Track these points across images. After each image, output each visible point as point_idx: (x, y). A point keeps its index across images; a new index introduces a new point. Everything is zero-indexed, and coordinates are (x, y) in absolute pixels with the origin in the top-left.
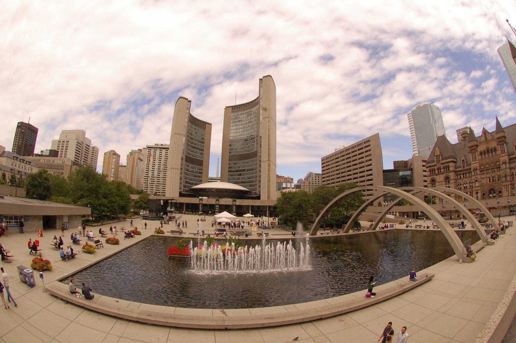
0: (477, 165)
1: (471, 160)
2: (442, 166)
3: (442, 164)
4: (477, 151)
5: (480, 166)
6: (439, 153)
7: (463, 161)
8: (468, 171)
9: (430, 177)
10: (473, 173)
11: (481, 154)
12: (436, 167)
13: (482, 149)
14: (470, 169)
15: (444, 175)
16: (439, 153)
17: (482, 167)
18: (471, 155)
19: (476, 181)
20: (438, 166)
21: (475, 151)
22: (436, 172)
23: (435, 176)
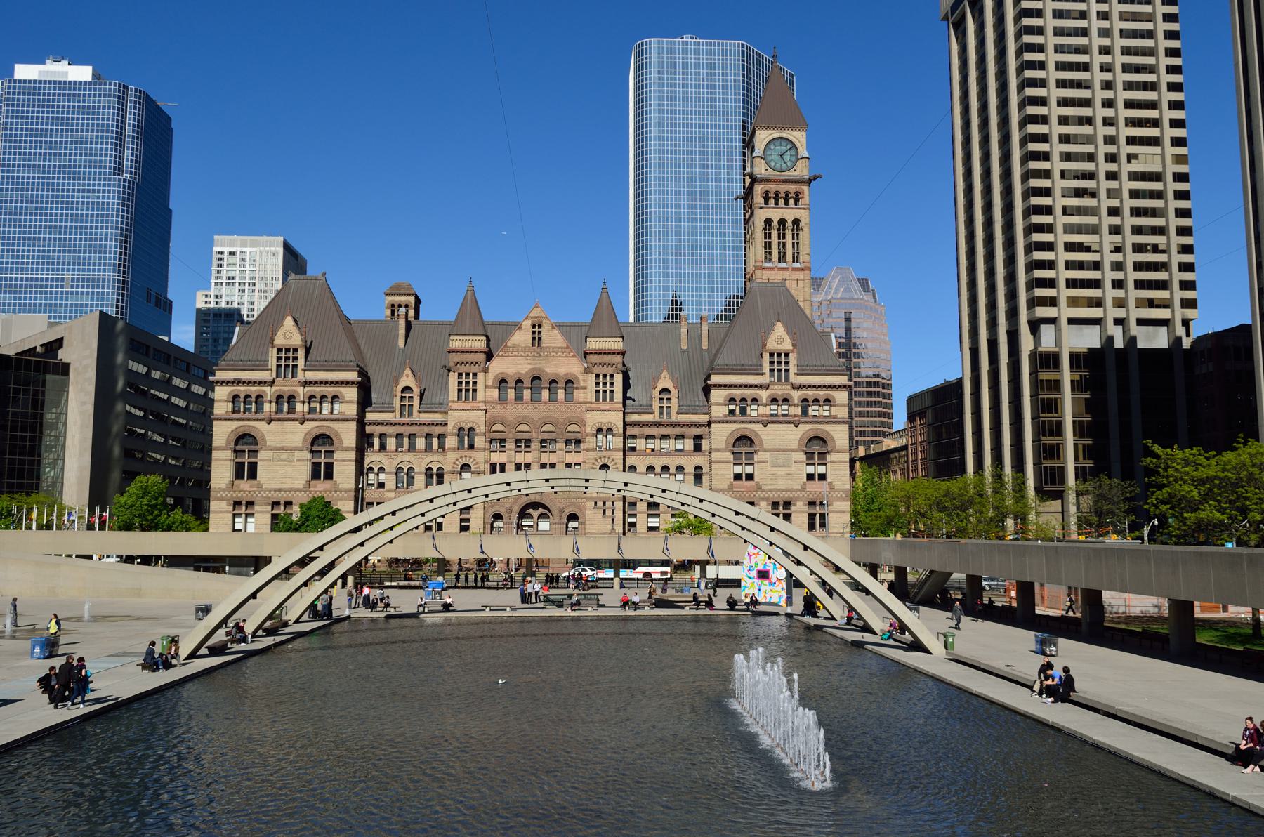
1: (453, 395)
2: (302, 392)
3: (306, 383)
4: (486, 371)
5: (489, 424)
6: (296, 340)
7: (407, 389)
8: (427, 429)
10: (451, 442)
12: (267, 389)
15: (309, 425)
16: (296, 340)
18: (453, 378)
19: (465, 467)
20: (284, 386)
21: (473, 369)
22: (269, 408)
23: (261, 426)
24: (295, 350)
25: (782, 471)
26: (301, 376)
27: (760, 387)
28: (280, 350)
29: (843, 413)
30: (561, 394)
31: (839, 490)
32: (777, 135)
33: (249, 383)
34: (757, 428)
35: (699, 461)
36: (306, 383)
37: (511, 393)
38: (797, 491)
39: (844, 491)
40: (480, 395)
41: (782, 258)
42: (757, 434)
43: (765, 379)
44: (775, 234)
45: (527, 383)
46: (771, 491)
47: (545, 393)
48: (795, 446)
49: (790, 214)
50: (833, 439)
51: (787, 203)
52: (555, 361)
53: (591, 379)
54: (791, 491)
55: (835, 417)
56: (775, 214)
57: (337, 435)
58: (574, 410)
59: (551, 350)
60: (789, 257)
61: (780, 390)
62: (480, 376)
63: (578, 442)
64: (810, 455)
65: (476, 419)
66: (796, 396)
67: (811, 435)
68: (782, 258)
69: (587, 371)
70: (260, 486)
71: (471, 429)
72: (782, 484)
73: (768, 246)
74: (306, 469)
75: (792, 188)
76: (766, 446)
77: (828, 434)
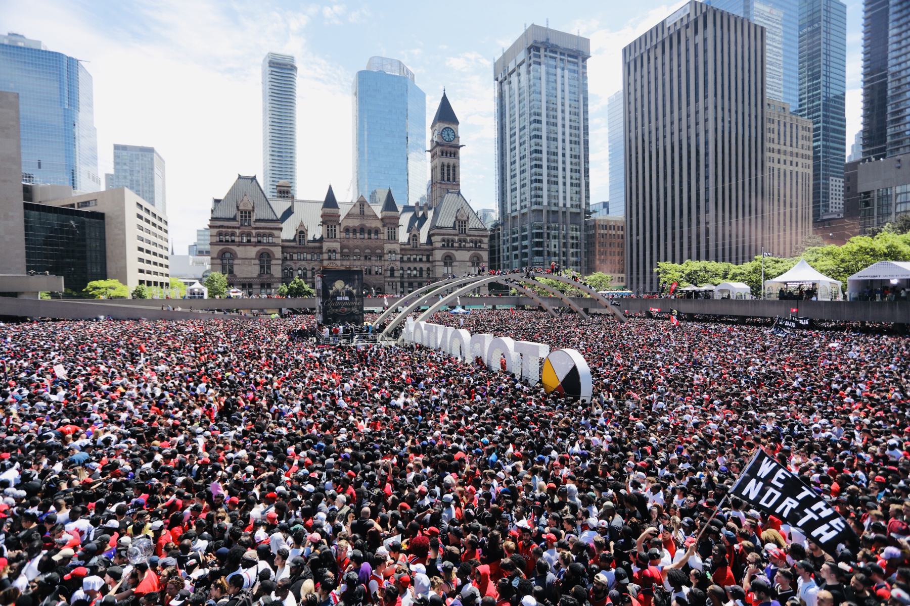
0: (337, 246)
2: (254, 232)
3: (256, 228)
5: (342, 248)
9: (221, 247)
11: (347, 230)
13: (351, 225)
14: (321, 248)
15: (258, 248)
17: (346, 250)
21: (335, 224)
24: (250, 213)
26: (253, 225)
27: (455, 235)
28: (242, 212)
29: (485, 246)
30: (373, 235)
32: (447, 126)
33: (228, 227)
35: (428, 265)
36: (256, 228)
37: (351, 235)
40: (338, 236)
41: (448, 179)
43: (457, 232)
44: (446, 169)
45: (358, 230)
47: (366, 236)
49: (451, 161)
52: (370, 222)
53: (386, 230)
57: (272, 252)
58: (379, 243)
59: (368, 216)
60: (451, 179)
61: (462, 237)
62: (337, 227)
63: (381, 257)
65: (337, 246)
66: (468, 239)
68: (448, 179)
69: (384, 226)
70: (235, 276)
71: (334, 251)
73: (443, 174)
74: (258, 268)
75: (453, 150)
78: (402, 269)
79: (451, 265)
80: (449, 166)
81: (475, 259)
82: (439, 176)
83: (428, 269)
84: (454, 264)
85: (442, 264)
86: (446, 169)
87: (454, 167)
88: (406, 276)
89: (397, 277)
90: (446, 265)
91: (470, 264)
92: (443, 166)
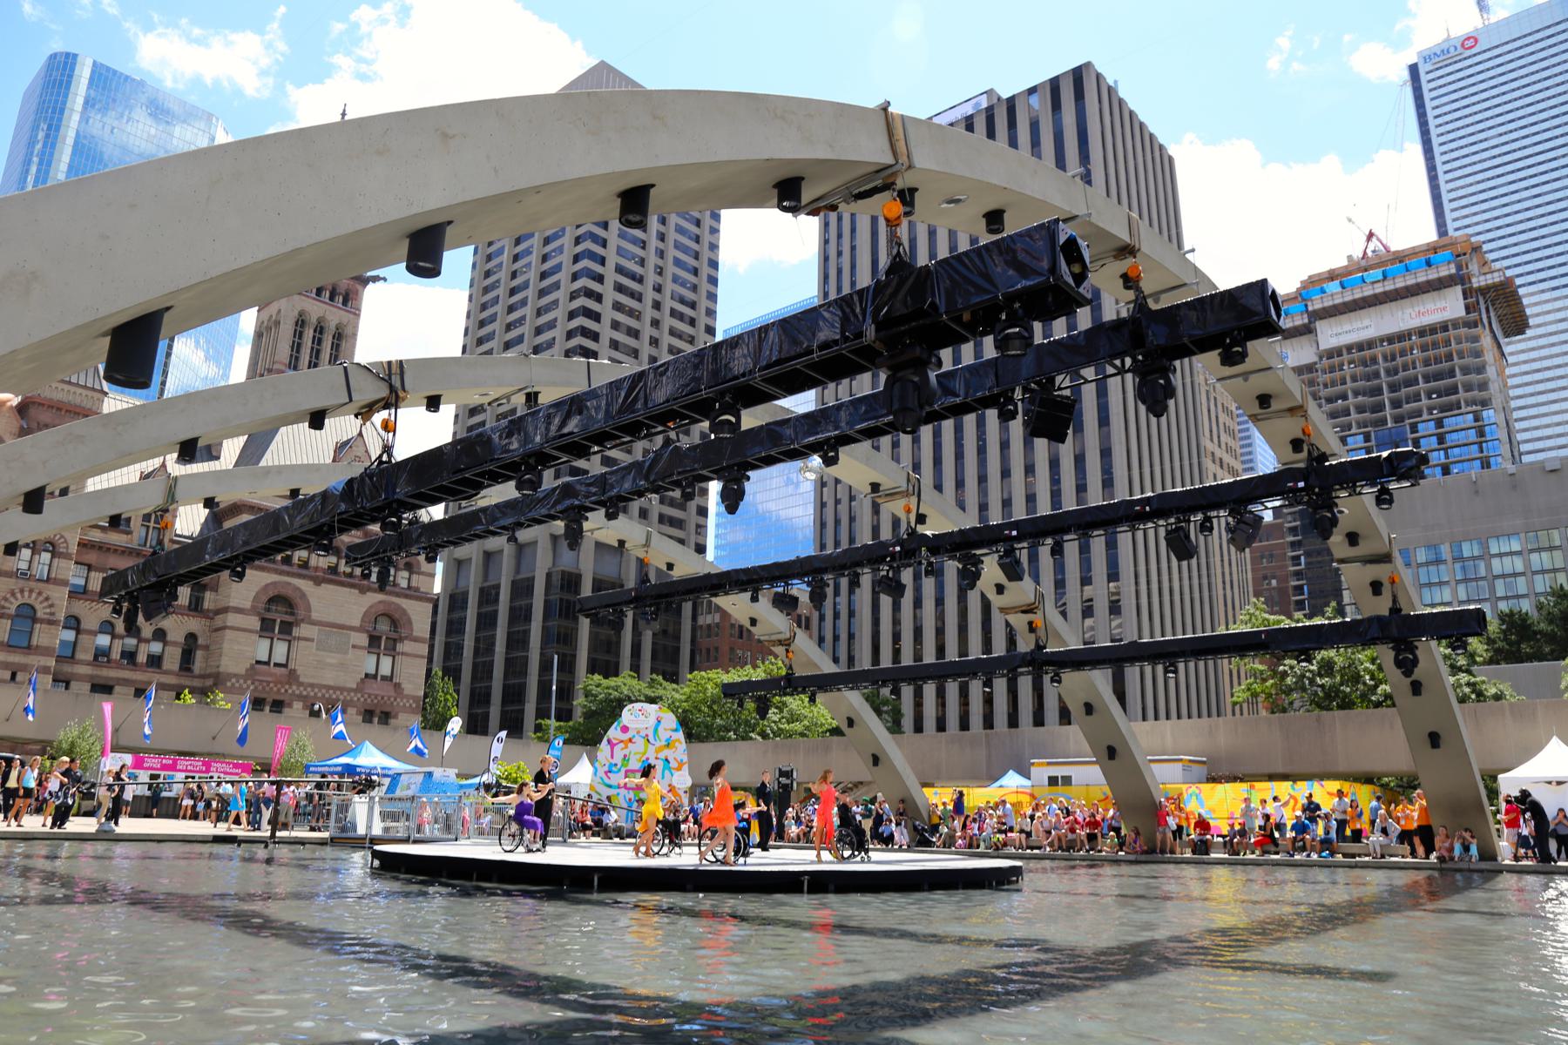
25: (332, 659)
31: (408, 697)
34: (305, 585)
35: (194, 624)
38: (350, 690)
39: (415, 698)
42: (303, 596)
44: (309, 334)
46: (312, 686)
48: (356, 623)
50: (410, 622)
51: (332, 298)
54: (342, 689)
55: (417, 589)
56: (316, 309)
64: (374, 640)
67: (381, 609)
72: (329, 678)
73: (297, 347)
76: (315, 616)
77: (404, 612)
78: (74, 623)
79: (287, 628)
80: (320, 329)
81: (384, 627)
82: (284, 351)
83: (191, 637)
84: (302, 630)
85: (254, 623)
86: (309, 334)
87: (339, 336)
88: (85, 655)
89: (47, 651)
90: (266, 627)
91: (363, 639)
92: (301, 323)
